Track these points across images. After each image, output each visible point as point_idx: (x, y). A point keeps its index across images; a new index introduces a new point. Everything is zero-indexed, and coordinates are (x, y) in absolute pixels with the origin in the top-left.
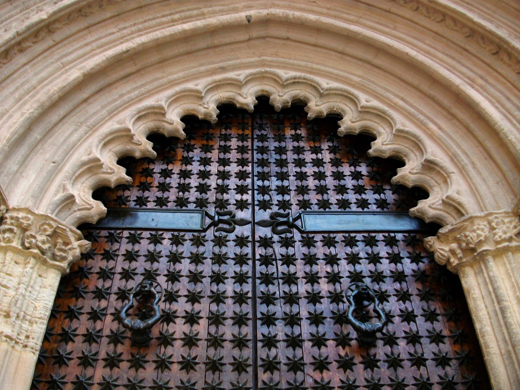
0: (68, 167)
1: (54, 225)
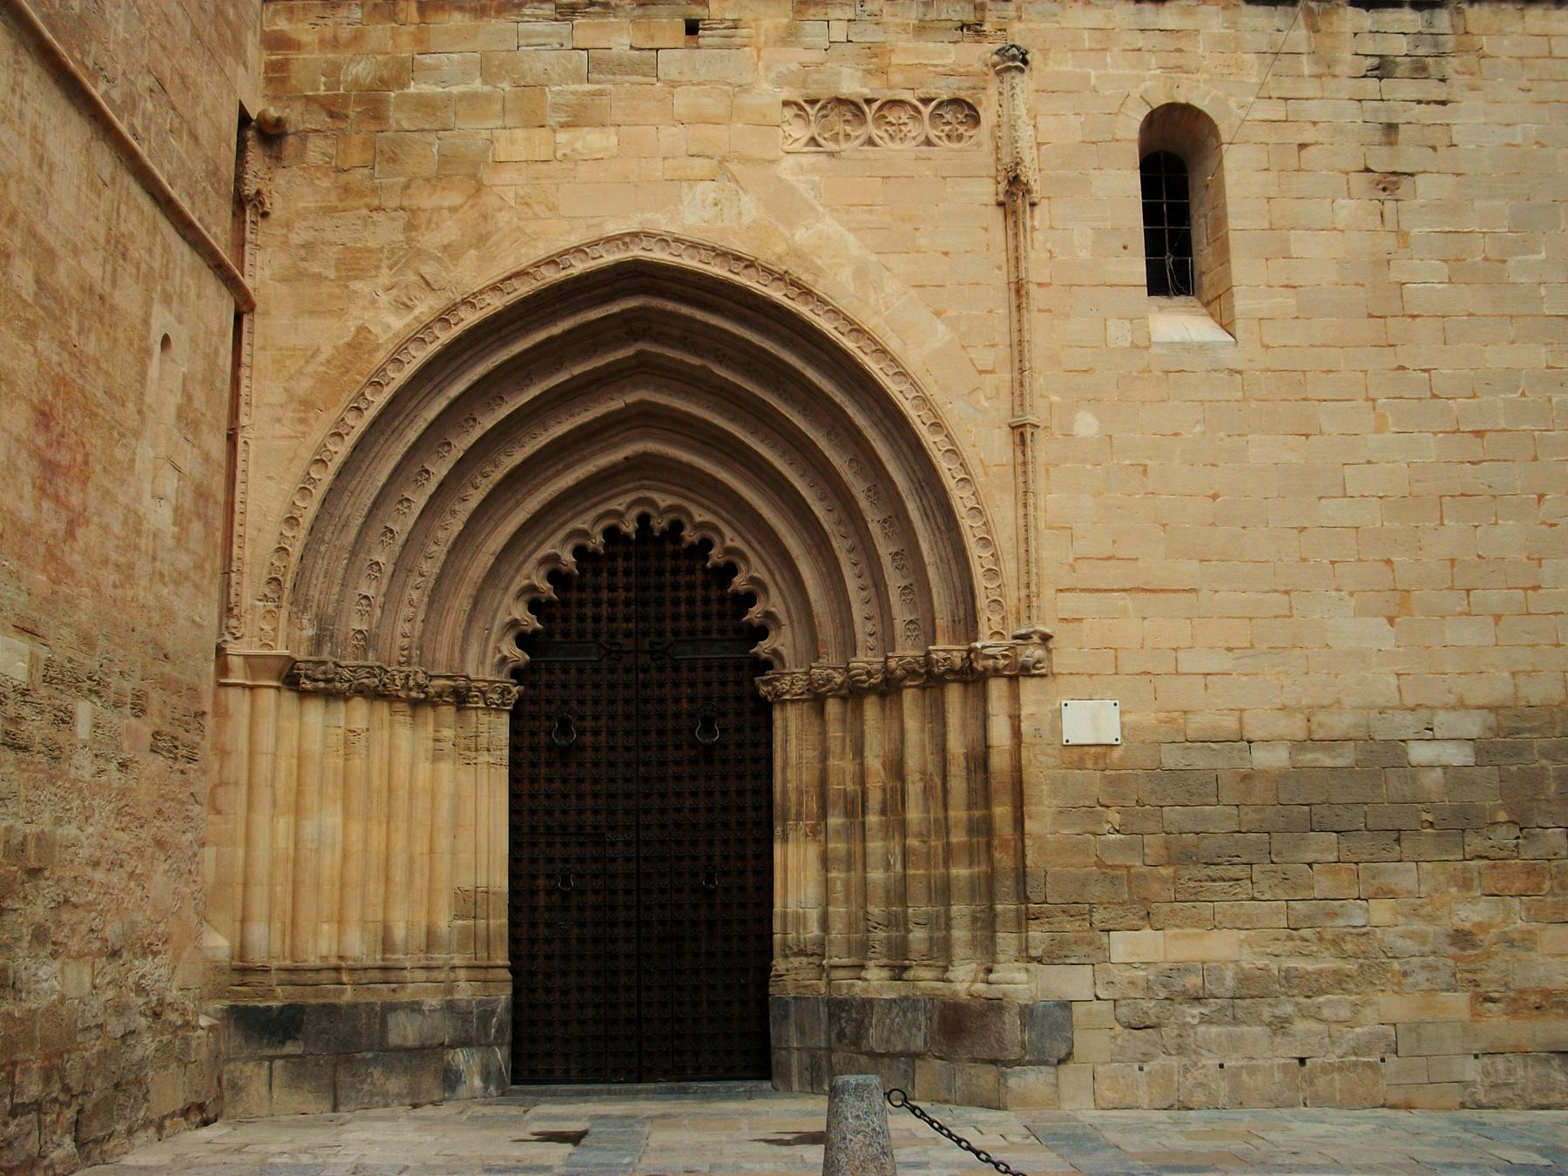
0: (496, 627)
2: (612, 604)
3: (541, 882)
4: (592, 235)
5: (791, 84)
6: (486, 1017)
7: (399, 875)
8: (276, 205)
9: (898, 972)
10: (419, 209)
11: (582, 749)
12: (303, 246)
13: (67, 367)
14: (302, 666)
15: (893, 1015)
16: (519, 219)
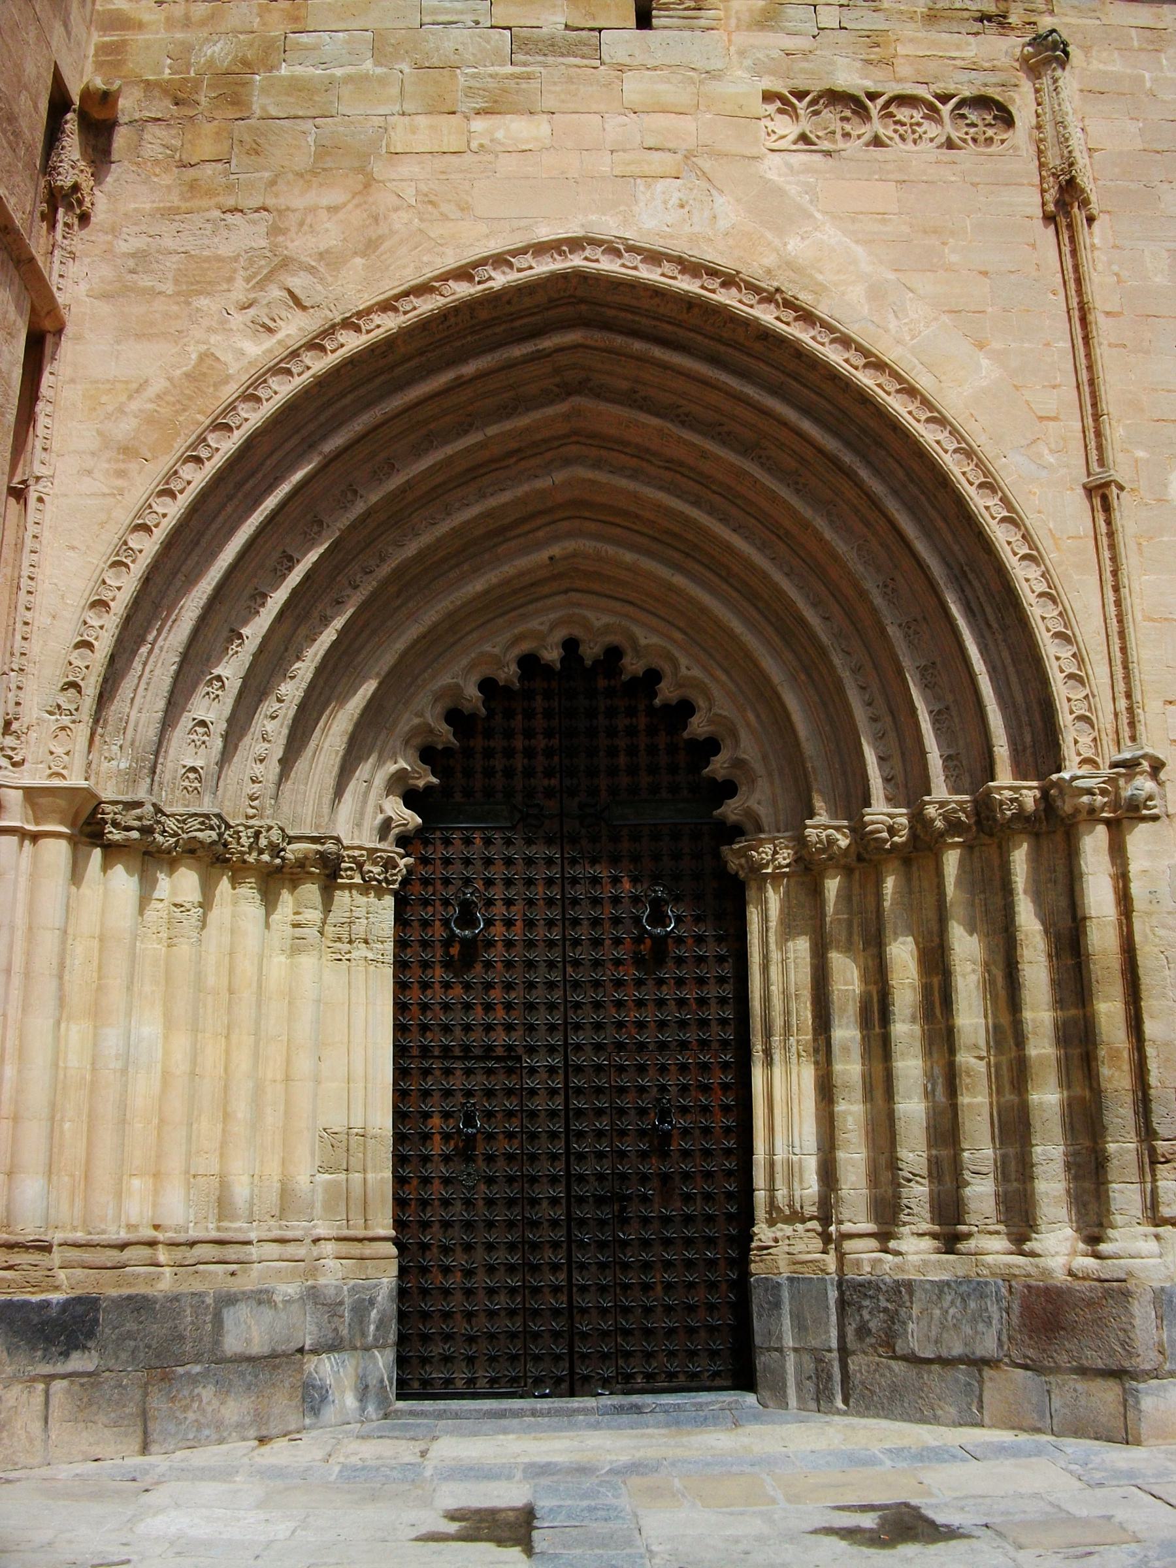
1: (384, 855)
2: (529, 753)
3: (436, 1121)
4: (518, 241)
5: (772, 73)
6: (361, 1309)
7: (241, 1109)
9: (950, 1241)
10: (288, 209)
11: (490, 944)
12: (133, 255)
14: (109, 808)
15: (946, 1304)
16: (421, 220)
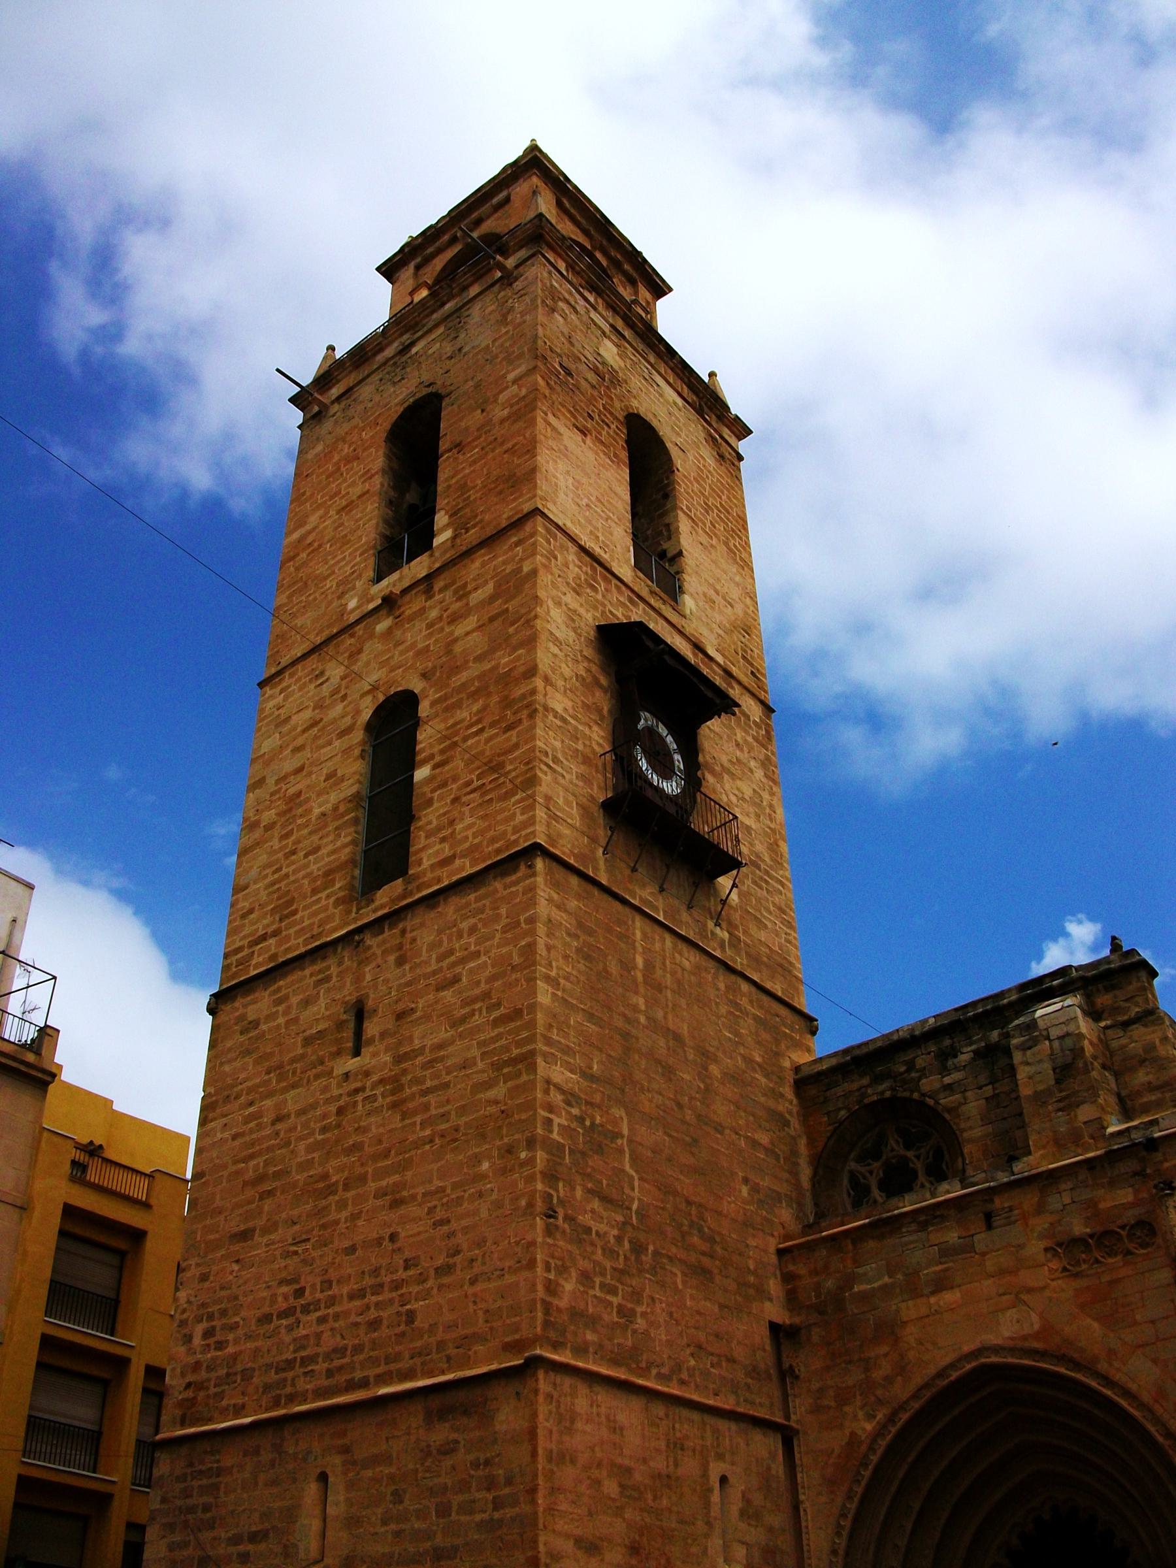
8: (802, 1371)
13: (648, 1520)
